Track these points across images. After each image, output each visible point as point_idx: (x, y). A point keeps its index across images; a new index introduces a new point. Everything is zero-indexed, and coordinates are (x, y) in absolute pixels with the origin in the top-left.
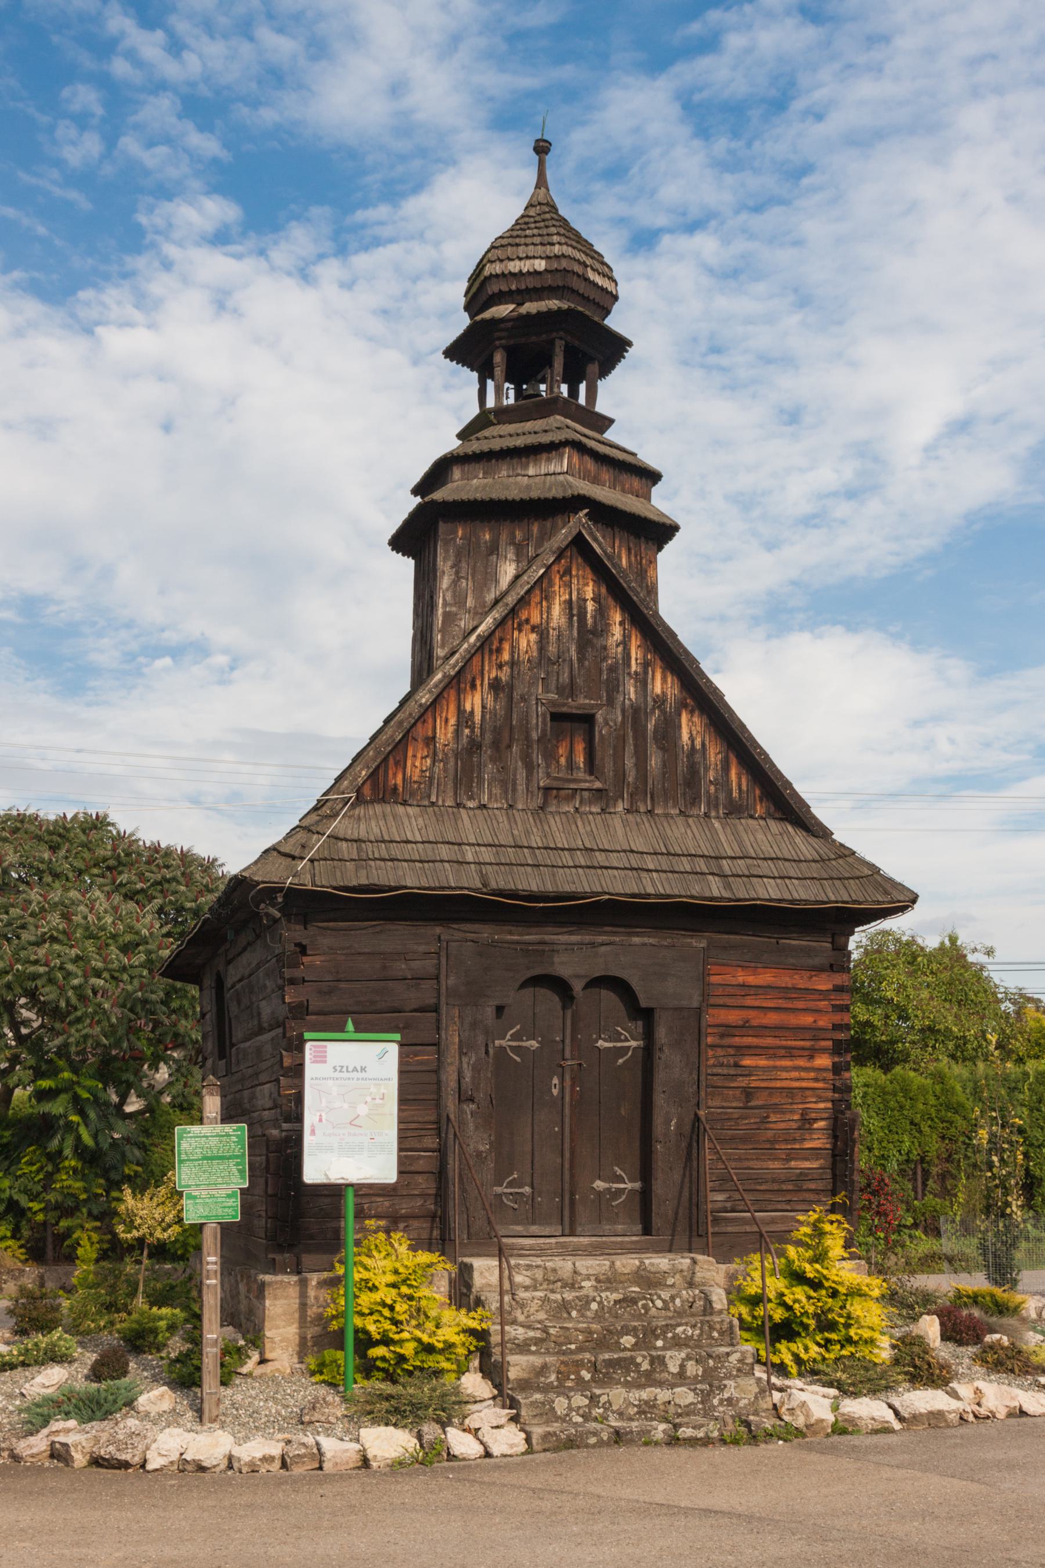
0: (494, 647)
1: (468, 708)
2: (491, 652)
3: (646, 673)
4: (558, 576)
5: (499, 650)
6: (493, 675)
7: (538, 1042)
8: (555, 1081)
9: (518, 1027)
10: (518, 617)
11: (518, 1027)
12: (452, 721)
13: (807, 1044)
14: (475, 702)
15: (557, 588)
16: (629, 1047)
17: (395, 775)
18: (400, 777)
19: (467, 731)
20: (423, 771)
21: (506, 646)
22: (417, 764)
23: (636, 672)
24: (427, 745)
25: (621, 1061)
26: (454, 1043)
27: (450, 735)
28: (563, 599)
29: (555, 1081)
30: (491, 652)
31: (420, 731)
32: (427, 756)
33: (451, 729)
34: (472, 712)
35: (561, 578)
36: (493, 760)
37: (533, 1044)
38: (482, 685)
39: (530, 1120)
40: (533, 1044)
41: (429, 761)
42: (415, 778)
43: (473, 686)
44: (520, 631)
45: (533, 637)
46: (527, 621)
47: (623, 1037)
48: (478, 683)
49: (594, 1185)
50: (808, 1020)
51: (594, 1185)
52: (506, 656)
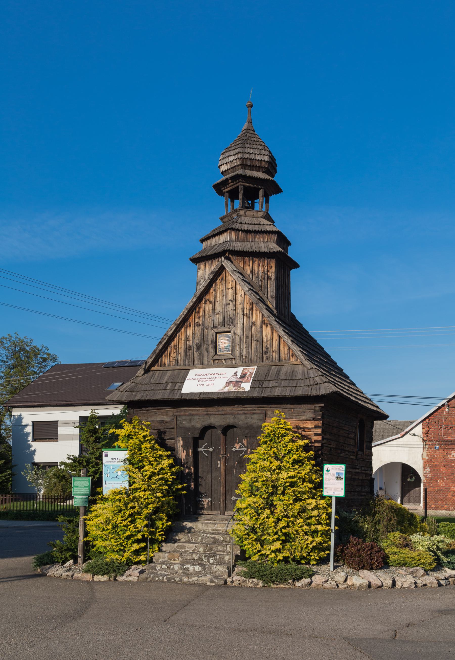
0: (197, 311)
1: (188, 334)
2: (196, 313)
3: (249, 313)
4: (219, 281)
5: (199, 312)
6: (197, 321)
7: (213, 449)
8: (219, 462)
9: (206, 444)
10: (205, 299)
11: (206, 444)
12: (183, 339)
14: (190, 332)
15: (219, 286)
17: (165, 360)
18: (166, 361)
19: (188, 342)
20: (173, 358)
21: (201, 310)
22: (172, 355)
23: (247, 314)
24: (175, 348)
25: (241, 455)
26: (180, 450)
27: (182, 344)
28: (221, 290)
29: (219, 462)
30: (196, 313)
31: (173, 344)
32: (175, 352)
33: (183, 342)
34: (189, 335)
35: (220, 282)
36: (197, 351)
37: (211, 450)
38: (193, 325)
39: (210, 475)
40: (211, 450)
41: (175, 354)
42: (171, 361)
43: (190, 326)
44: (205, 303)
45: (211, 305)
46: (209, 300)
47: (242, 447)
48: (192, 324)
49: (232, 498)
51: (232, 498)
52: (201, 314)
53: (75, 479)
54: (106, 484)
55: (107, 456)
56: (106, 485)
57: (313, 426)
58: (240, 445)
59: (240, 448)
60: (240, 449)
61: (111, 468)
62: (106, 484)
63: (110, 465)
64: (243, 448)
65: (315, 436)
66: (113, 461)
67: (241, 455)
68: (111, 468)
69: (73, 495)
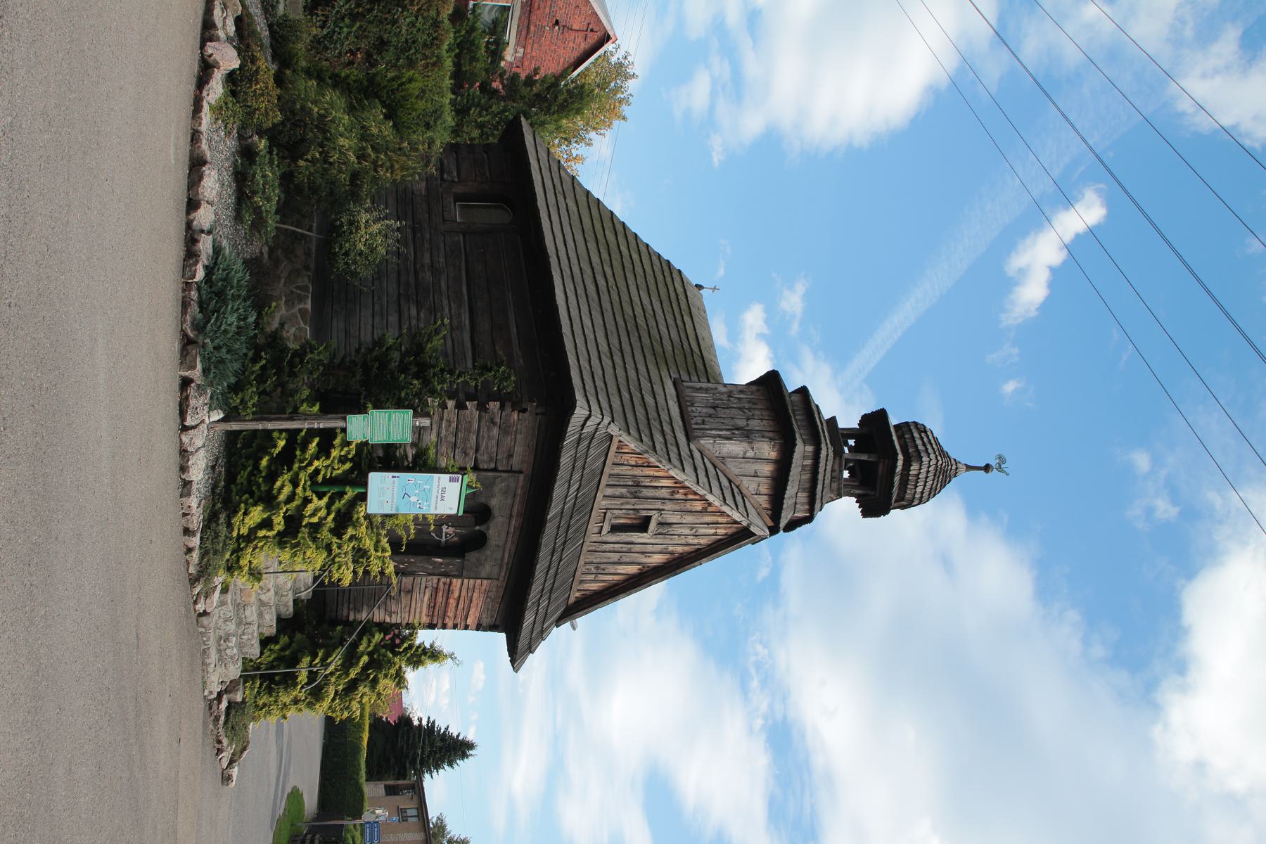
13: (436, 613)
16: (442, 538)
25: (434, 535)
50: (451, 613)
53: (408, 414)
54: (393, 477)
55: (451, 480)
56: (390, 477)
57: (468, 623)
58: (450, 535)
59: (446, 534)
60: (444, 534)
61: (425, 487)
62: (393, 477)
63: (432, 486)
64: (446, 537)
65: (454, 624)
66: (441, 488)
67: (434, 535)
68: (425, 487)
69: (372, 414)
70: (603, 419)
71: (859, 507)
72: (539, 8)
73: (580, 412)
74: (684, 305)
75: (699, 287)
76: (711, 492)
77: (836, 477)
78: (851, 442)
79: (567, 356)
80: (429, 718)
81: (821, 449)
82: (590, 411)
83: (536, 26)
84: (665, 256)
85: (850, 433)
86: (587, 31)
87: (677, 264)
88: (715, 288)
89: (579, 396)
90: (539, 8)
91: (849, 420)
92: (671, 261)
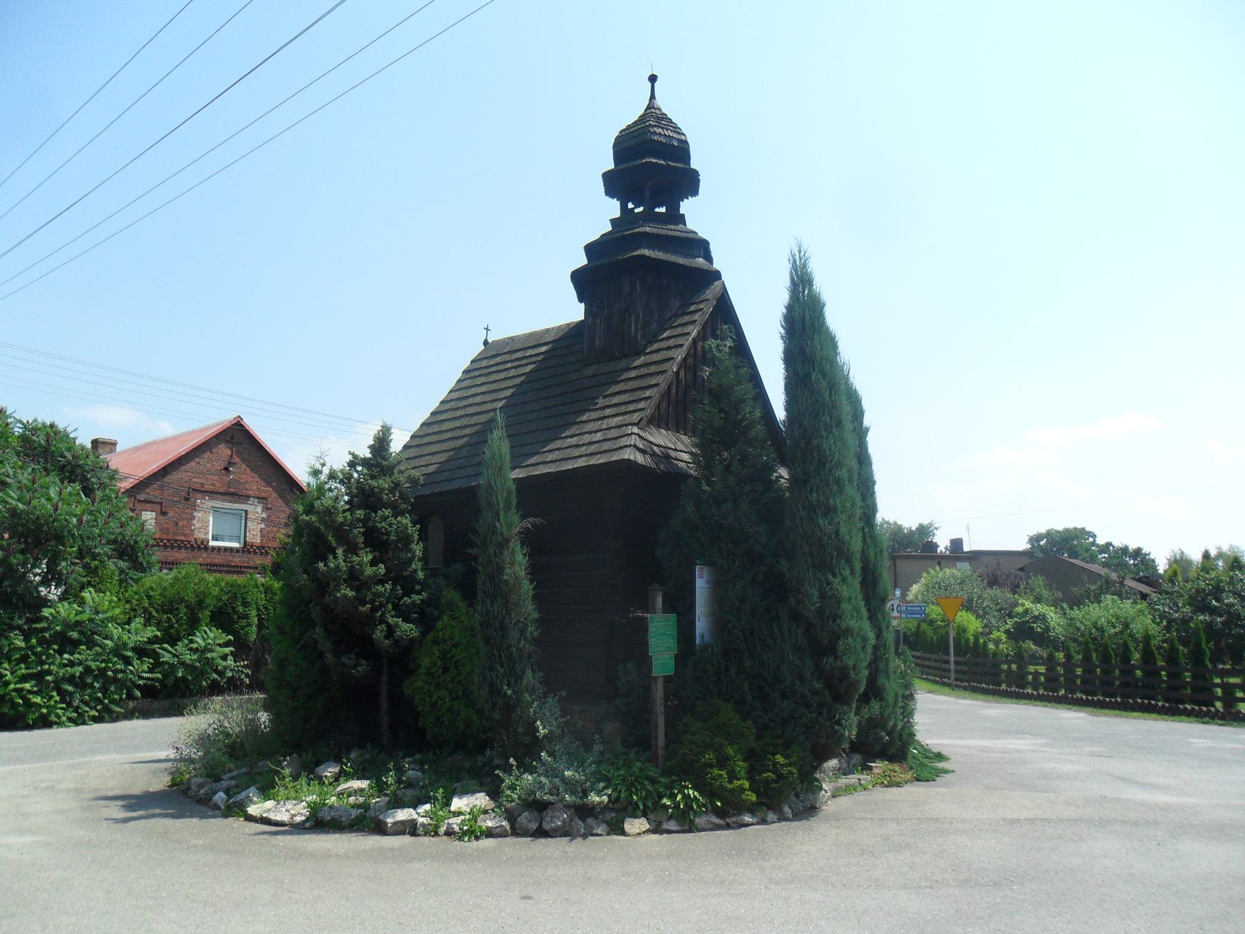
70: (635, 434)
71: (688, 199)
72: (214, 485)
73: (628, 454)
74: (506, 357)
75: (486, 343)
76: (688, 334)
77: (661, 219)
78: (630, 205)
79: (578, 467)
80: (15, 412)
81: (645, 233)
82: (630, 446)
83: (230, 488)
84: (459, 375)
85: (624, 208)
86: (232, 442)
87: (466, 364)
88: (487, 329)
89: (615, 457)
90: (214, 485)
91: (613, 208)
92: (463, 369)
